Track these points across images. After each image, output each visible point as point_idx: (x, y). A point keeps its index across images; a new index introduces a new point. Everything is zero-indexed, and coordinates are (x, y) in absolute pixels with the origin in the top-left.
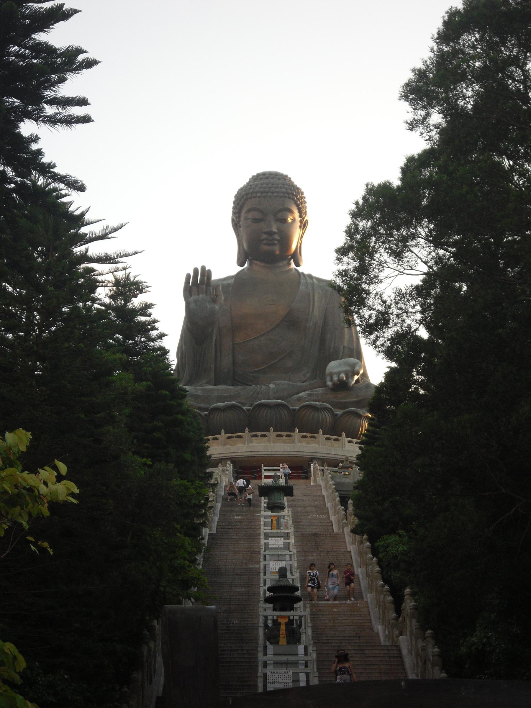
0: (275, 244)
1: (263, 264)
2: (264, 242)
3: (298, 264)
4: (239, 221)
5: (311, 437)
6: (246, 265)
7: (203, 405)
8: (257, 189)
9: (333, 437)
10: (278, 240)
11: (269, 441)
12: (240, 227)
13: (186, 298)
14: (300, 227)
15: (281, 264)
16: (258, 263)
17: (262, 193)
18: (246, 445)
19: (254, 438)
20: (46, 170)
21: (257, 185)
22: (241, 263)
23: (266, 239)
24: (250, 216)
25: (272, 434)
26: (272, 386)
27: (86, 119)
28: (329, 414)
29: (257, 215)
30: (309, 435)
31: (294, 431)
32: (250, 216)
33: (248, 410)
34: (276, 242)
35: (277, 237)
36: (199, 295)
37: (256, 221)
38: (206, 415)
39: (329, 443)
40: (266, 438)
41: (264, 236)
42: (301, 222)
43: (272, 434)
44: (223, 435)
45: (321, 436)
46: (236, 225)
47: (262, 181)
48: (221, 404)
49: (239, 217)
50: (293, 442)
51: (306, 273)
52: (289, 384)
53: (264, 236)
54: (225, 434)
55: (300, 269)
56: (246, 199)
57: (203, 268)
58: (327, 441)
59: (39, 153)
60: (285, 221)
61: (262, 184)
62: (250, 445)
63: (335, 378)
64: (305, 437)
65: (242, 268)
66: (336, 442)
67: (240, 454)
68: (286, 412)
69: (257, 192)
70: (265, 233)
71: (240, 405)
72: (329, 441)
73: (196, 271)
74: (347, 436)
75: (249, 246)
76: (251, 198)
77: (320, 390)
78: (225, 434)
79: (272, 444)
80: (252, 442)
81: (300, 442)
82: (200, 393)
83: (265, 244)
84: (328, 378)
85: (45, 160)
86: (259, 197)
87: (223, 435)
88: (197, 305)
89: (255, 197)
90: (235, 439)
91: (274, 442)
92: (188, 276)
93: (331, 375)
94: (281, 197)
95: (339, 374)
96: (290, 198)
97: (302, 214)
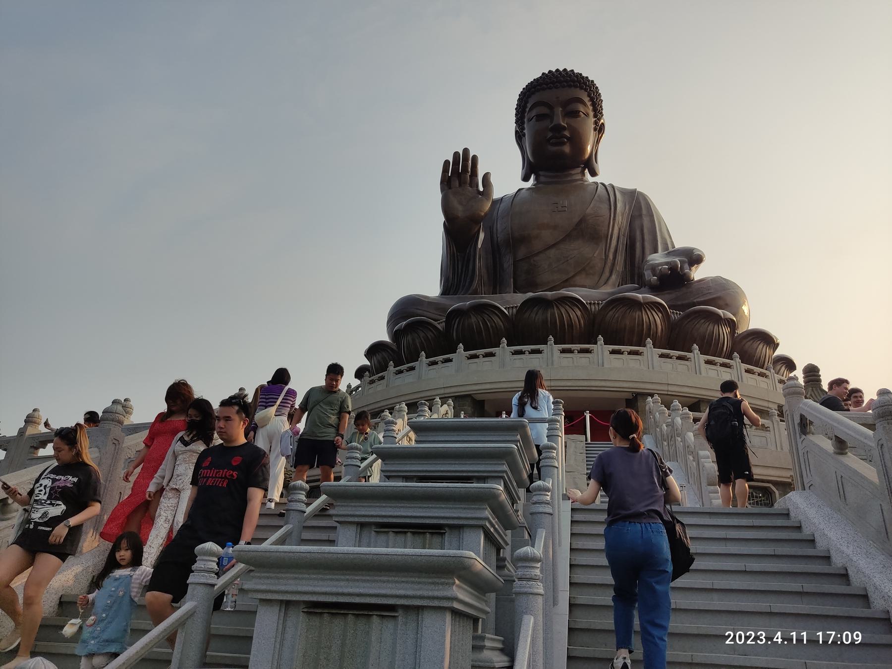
0: (563, 144)
3: (594, 173)
4: (523, 129)
10: (568, 139)
12: (524, 135)
14: (595, 129)
15: (573, 172)
19: (515, 357)
22: (526, 179)
23: (551, 138)
24: (534, 113)
28: (660, 315)
29: (543, 110)
31: (596, 343)
32: (534, 113)
35: (567, 133)
37: (540, 117)
39: (668, 364)
41: (550, 134)
42: (596, 123)
45: (650, 351)
46: (519, 137)
49: (523, 123)
53: (550, 134)
54: (465, 350)
56: (529, 97)
57: (466, 151)
60: (575, 114)
67: (488, 386)
68: (579, 313)
73: (456, 154)
74: (703, 352)
75: (534, 153)
76: (533, 93)
92: (447, 163)
93: (653, 268)
95: (667, 263)
96: (581, 88)
97: (598, 111)
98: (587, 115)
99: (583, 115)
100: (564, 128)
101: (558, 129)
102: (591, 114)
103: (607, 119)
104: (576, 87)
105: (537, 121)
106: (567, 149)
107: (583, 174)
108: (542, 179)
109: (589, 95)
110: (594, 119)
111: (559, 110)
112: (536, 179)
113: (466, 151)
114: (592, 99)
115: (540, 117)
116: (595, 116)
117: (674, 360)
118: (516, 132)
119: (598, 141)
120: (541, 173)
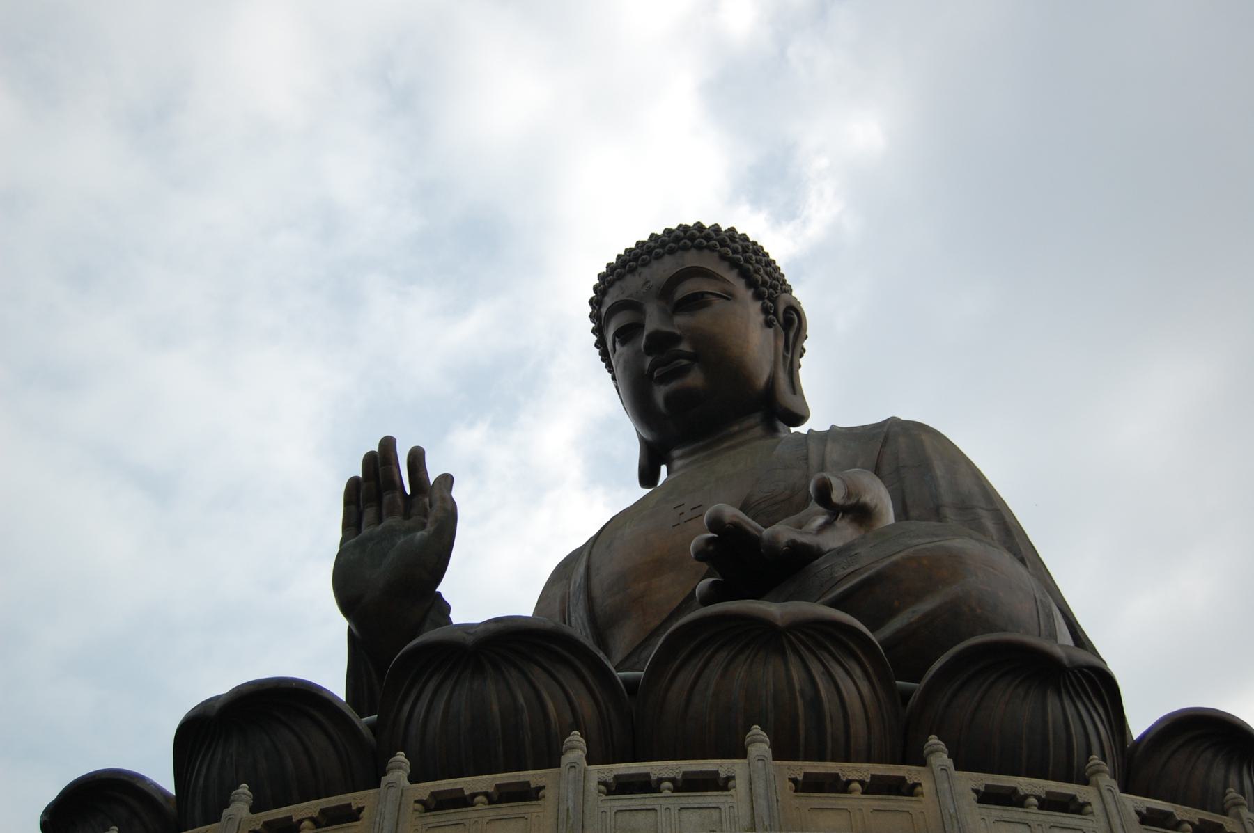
0: (681, 372)
10: (693, 358)
14: (769, 324)
15: (736, 428)
23: (654, 367)
34: (684, 362)
35: (685, 347)
42: (765, 310)
53: (648, 361)
55: (803, 429)
57: (388, 444)
66: (505, 809)
70: (649, 350)
73: (371, 461)
83: (663, 380)
94: (671, 252)
96: (700, 248)
98: (728, 296)
99: (717, 301)
100: (673, 339)
101: (661, 343)
103: (801, 293)
104: (685, 248)
105: (623, 343)
106: (695, 379)
107: (772, 430)
108: (678, 464)
109: (723, 257)
112: (669, 473)
113: (388, 444)
114: (734, 264)
115: (625, 335)
116: (758, 296)
120: (676, 453)
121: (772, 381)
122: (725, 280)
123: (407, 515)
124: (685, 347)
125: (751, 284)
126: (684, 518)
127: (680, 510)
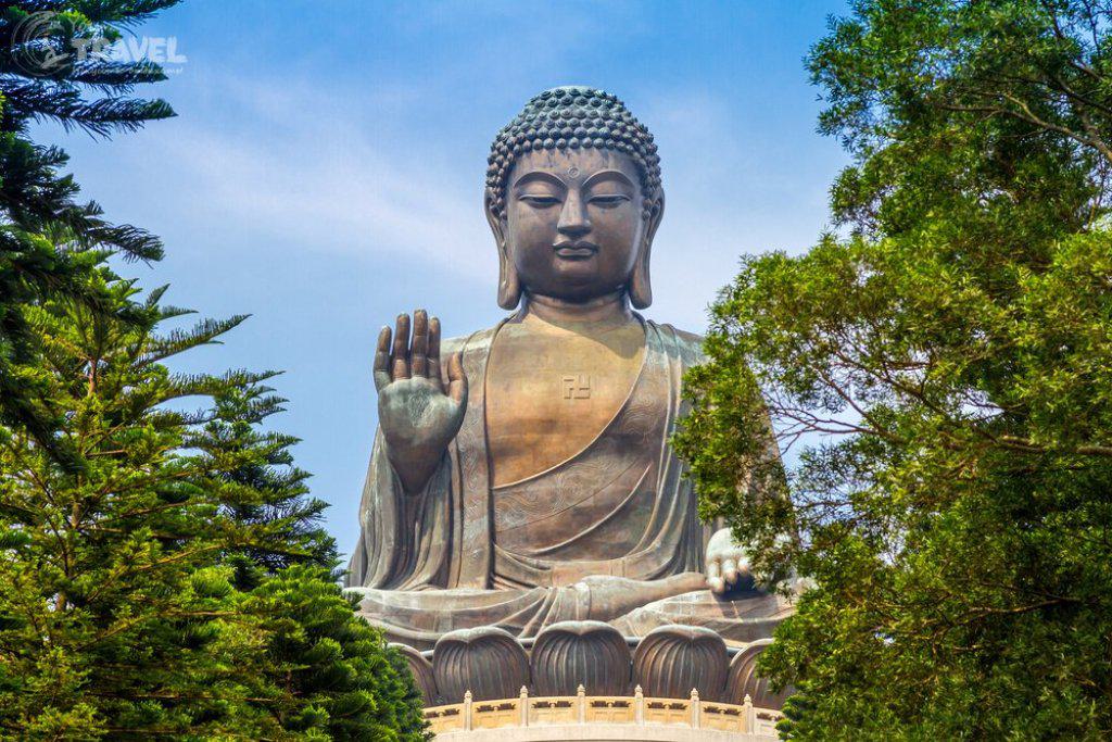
1: (558, 303)
2: (561, 252)
5: (674, 707)
6: (520, 306)
7: (422, 634)
8: (544, 129)
9: (723, 706)
11: (576, 717)
13: (379, 385)
14: (644, 218)
15: (600, 302)
16: (549, 300)
17: (556, 137)
18: (523, 726)
19: (540, 711)
20: (83, 224)
21: (543, 118)
25: (581, 700)
26: (582, 587)
27: (159, 111)
30: (668, 701)
31: (633, 694)
33: (528, 646)
35: (589, 239)
36: (409, 377)
38: (429, 658)
40: (568, 710)
41: (560, 239)
43: (581, 700)
44: (468, 706)
47: (555, 110)
48: (464, 633)
50: (632, 718)
51: (659, 321)
52: (621, 584)
53: (560, 239)
58: (709, 715)
59: (67, 185)
61: (555, 117)
62: (531, 725)
63: (729, 570)
64: (660, 706)
65: (508, 314)
69: (544, 137)
70: (563, 231)
71: (508, 634)
72: (715, 715)
73: (404, 324)
77: (694, 597)
78: (474, 700)
79: (583, 724)
80: (536, 719)
81: (646, 717)
82: (414, 605)
83: (564, 258)
84: (712, 569)
85: (79, 200)
86: (550, 147)
87: (468, 706)
88: (405, 400)
89: (539, 148)
90: (495, 713)
91: (587, 719)
93: (719, 561)
101: (574, 232)
102: (638, 188)
107: (622, 305)
110: (641, 198)
111: (573, 197)
117: (722, 716)
118: (488, 201)
119: (650, 234)
121: (635, 267)
122: (632, 186)
123: (427, 376)
124: (589, 239)
125: (644, 185)
126: (574, 394)
127: (570, 385)
